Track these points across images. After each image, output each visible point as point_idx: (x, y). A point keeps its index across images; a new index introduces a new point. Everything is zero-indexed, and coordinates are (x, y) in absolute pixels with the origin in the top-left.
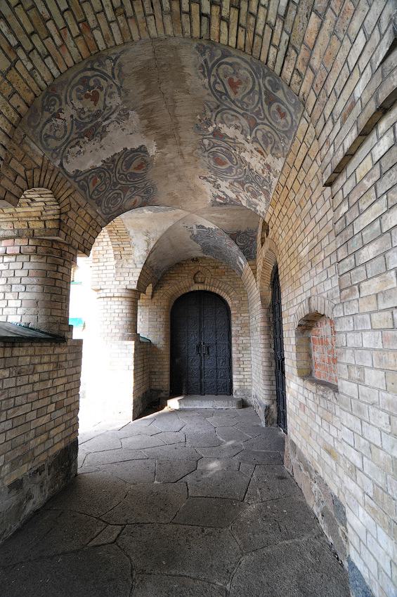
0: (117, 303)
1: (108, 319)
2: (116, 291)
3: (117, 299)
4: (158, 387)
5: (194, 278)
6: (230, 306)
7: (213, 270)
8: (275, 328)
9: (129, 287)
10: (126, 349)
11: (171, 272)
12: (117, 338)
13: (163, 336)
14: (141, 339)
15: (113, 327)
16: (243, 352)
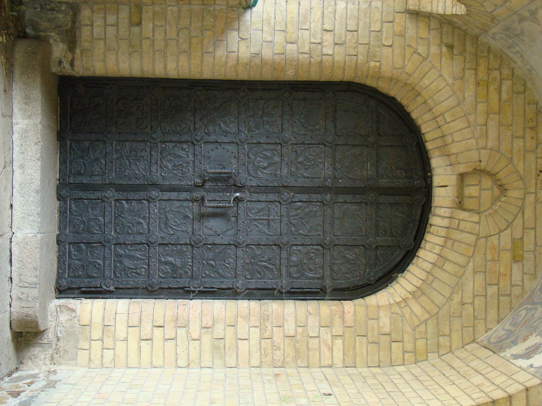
4: (85, 33)
5: (479, 172)
6: (372, 300)
7: (505, 239)
11: (506, 85)
13: (267, 53)
16: (206, 339)
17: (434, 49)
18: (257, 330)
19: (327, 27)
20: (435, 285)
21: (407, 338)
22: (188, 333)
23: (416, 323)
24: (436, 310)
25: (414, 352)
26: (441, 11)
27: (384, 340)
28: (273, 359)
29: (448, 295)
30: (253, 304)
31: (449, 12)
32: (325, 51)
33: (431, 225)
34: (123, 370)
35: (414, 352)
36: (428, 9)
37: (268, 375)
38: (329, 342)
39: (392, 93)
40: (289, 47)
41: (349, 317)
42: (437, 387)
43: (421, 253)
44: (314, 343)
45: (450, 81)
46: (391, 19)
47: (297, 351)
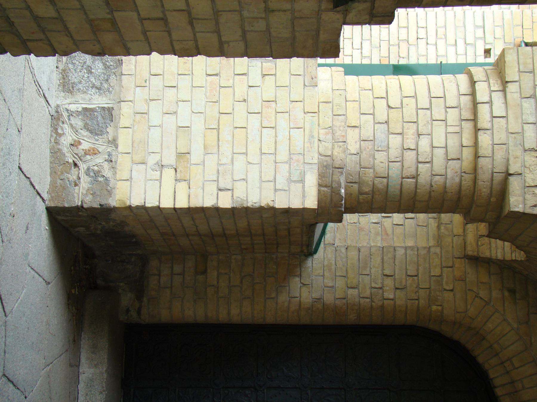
0: (453, 142)
1: (394, 114)
2: (500, 136)
3: (467, 140)
9: (514, 184)
10: (290, 181)
12: (326, 147)
13: (329, 298)
14: (320, 226)
15: (368, 133)
17: (496, 294)
19: (387, 272)
26: (500, 257)
31: (508, 257)
32: (386, 295)
36: (487, 254)
39: (456, 337)
40: (351, 292)
45: (515, 326)
46: (450, 264)
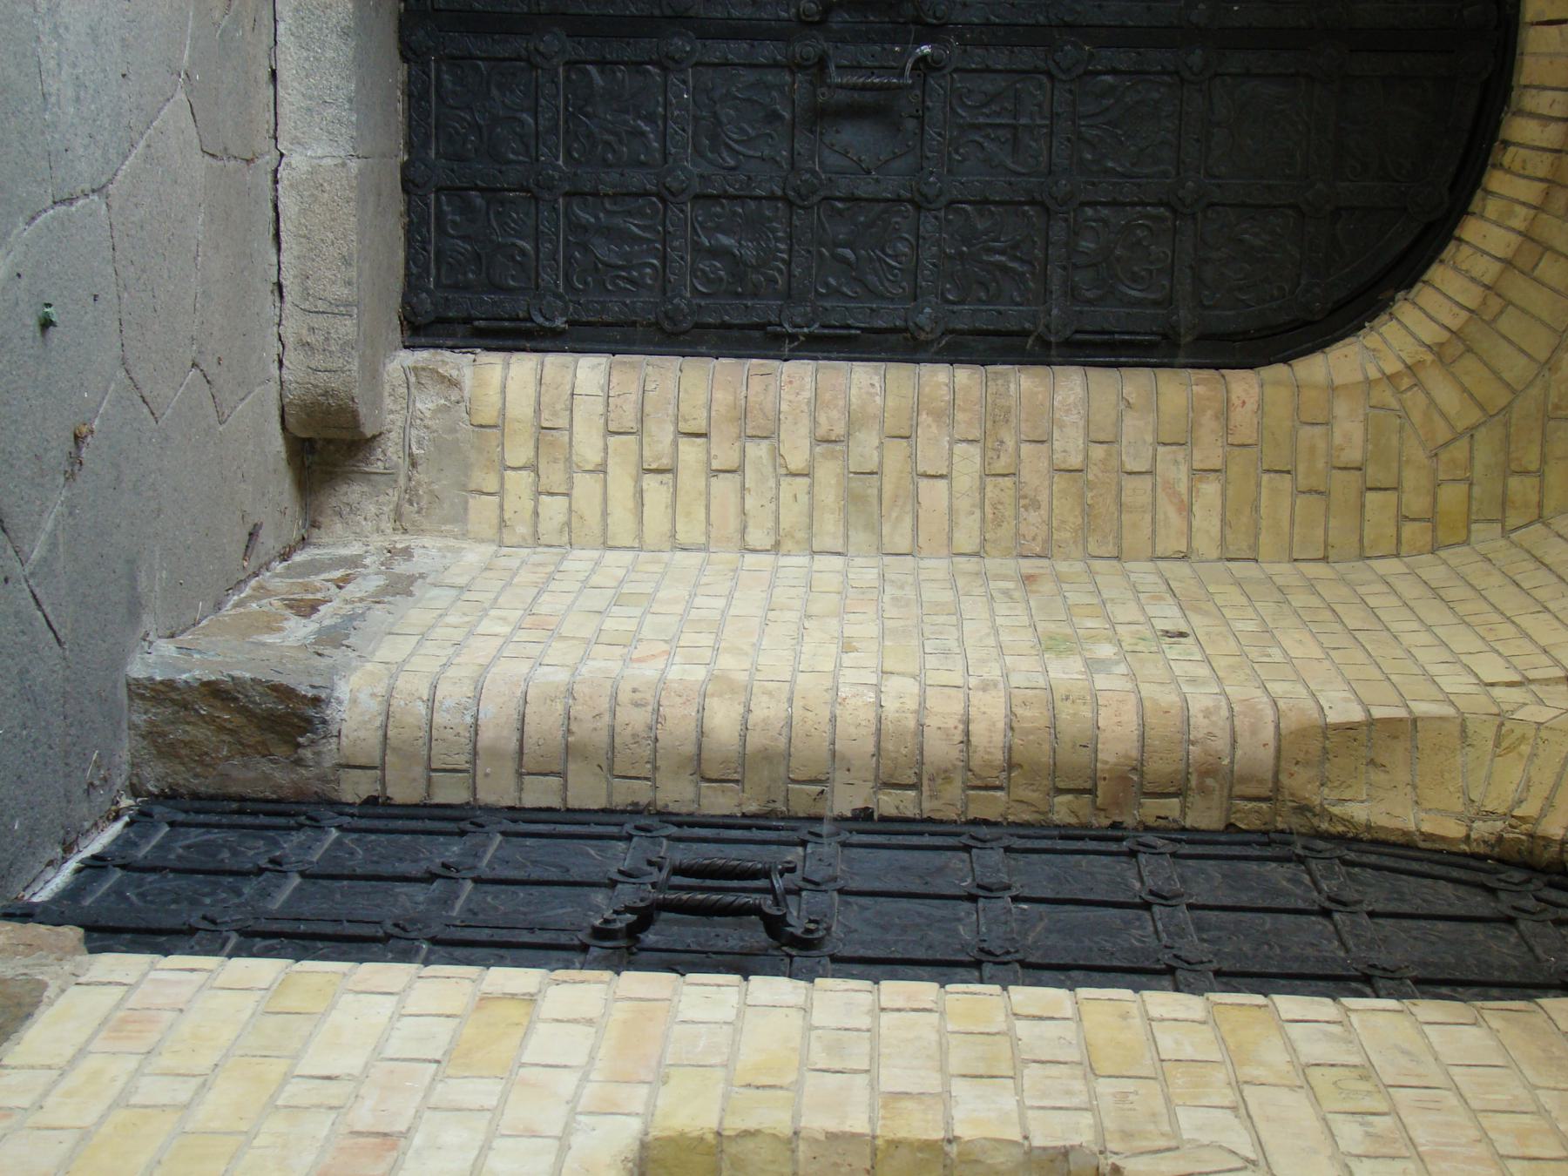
6: (1314, 368)
8: (1072, 837)
16: (828, 473)
18: (975, 450)
20: (1504, 324)
21: (1410, 478)
22: (776, 454)
23: (1443, 434)
24: (1502, 398)
25: (1431, 518)
27: (1346, 486)
28: (1018, 534)
29: (1543, 355)
30: (965, 376)
33: (1506, 144)
34: (595, 554)
35: (1431, 518)
37: (1004, 578)
38: (1183, 488)
41: (1244, 420)
42: (1496, 617)
43: (1471, 230)
44: (1137, 491)
47: (1087, 511)
